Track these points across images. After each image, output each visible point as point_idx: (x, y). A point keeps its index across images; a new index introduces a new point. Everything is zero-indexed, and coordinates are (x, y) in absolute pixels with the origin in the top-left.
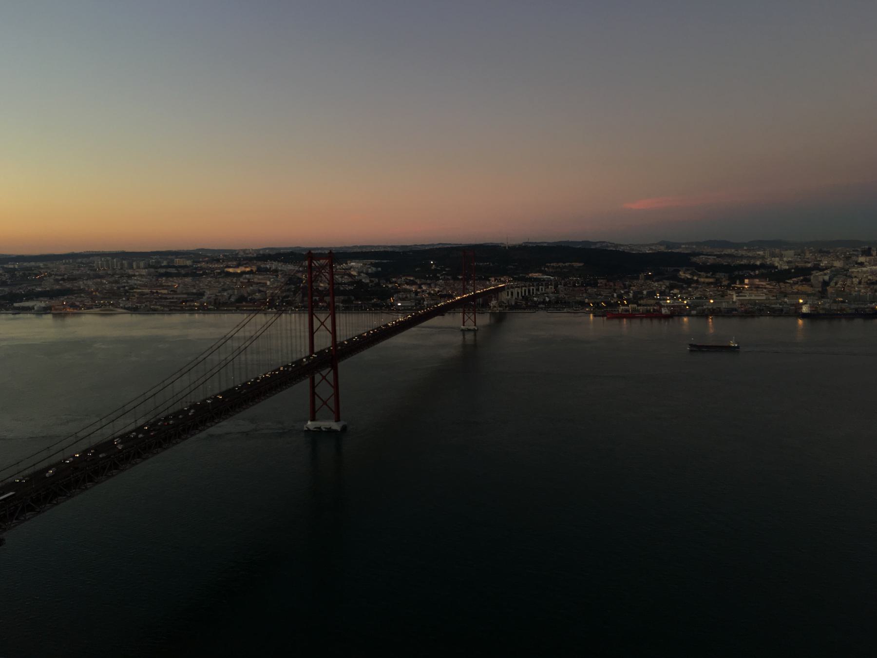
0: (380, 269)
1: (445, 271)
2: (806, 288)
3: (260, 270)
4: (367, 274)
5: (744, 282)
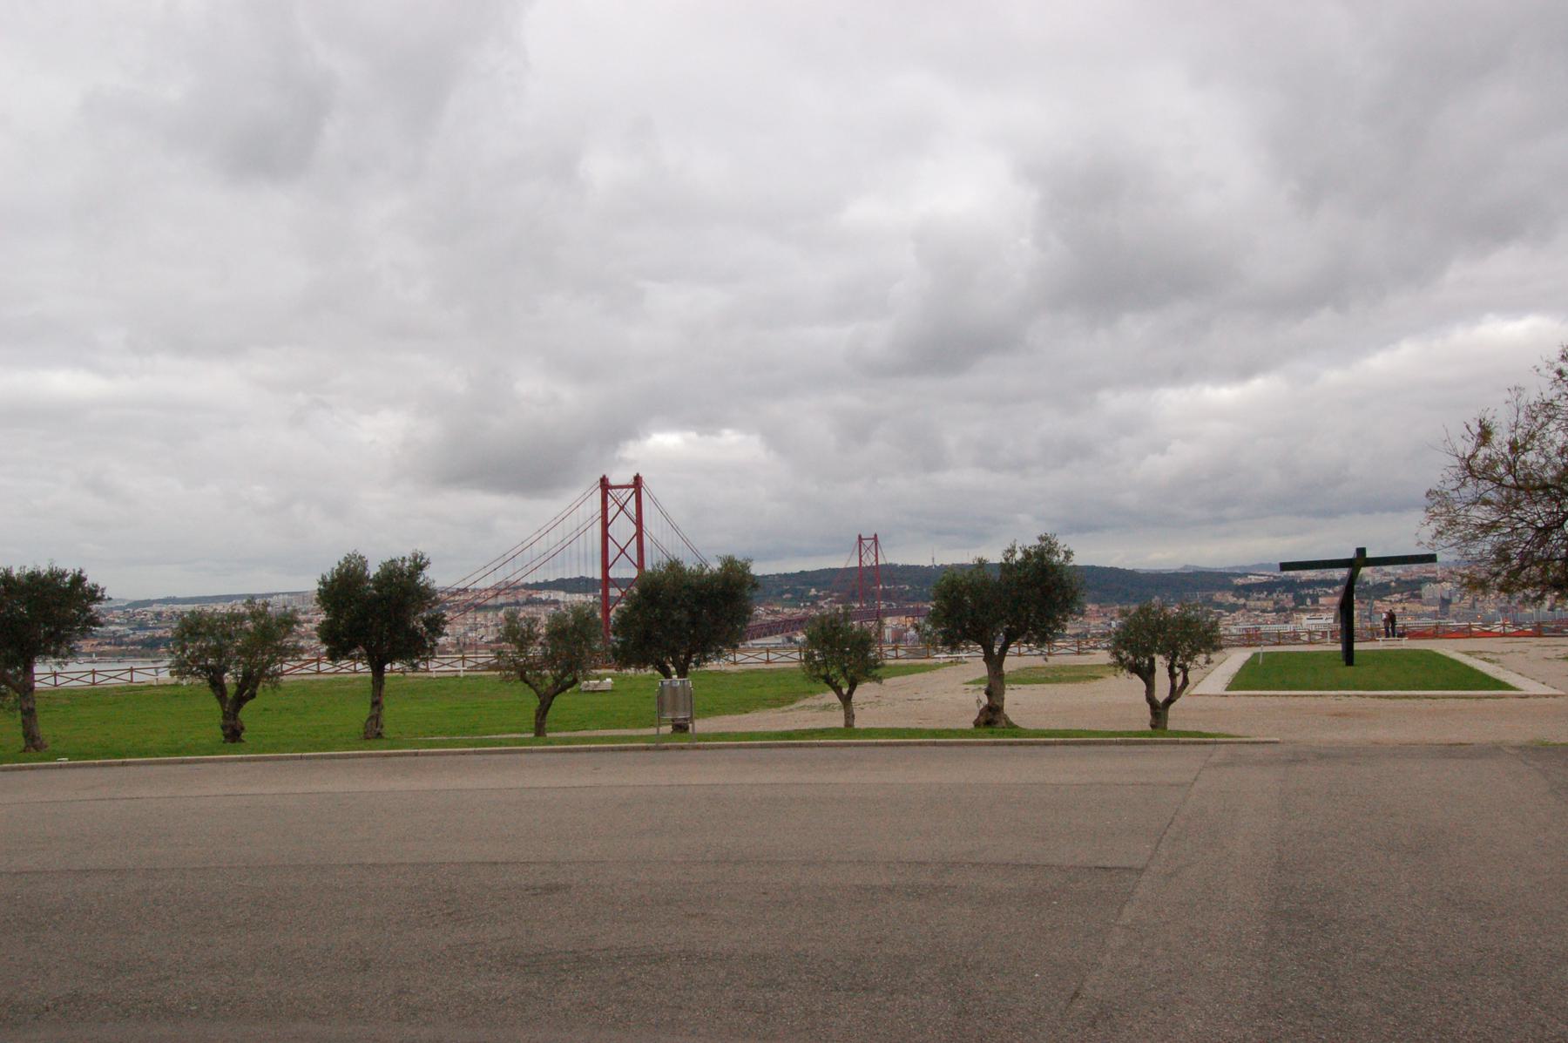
1: (831, 597)
3: (530, 602)
5: (1318, 602)
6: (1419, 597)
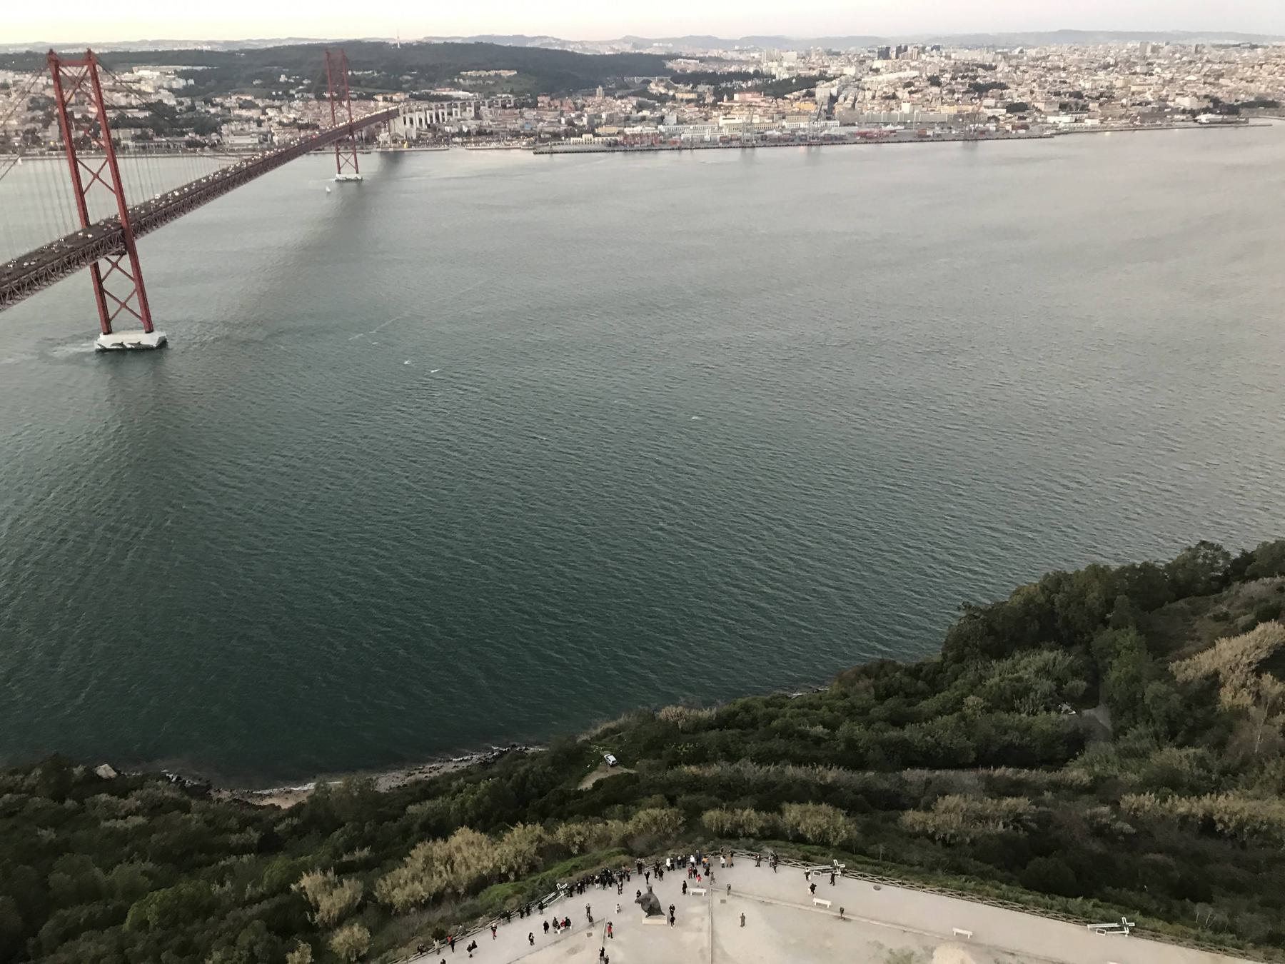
0: (191, 82)
1: (302, 84)
2: (809, 106)
4: (171, 90)
6: (812, 95)
